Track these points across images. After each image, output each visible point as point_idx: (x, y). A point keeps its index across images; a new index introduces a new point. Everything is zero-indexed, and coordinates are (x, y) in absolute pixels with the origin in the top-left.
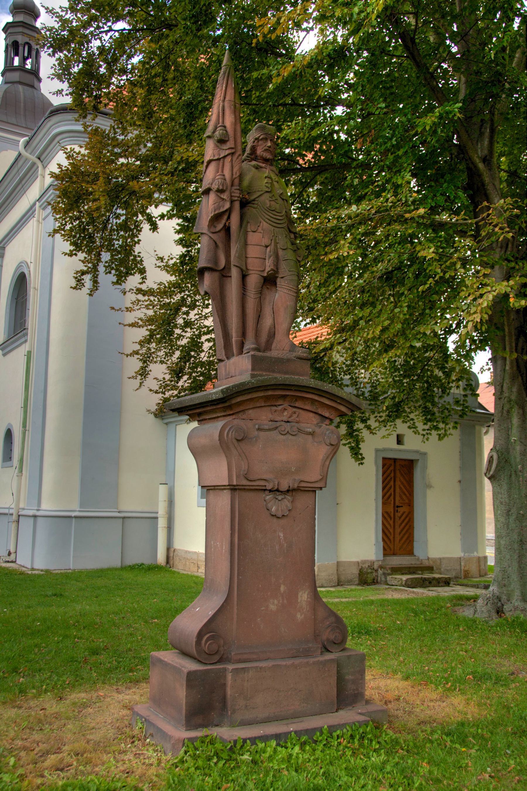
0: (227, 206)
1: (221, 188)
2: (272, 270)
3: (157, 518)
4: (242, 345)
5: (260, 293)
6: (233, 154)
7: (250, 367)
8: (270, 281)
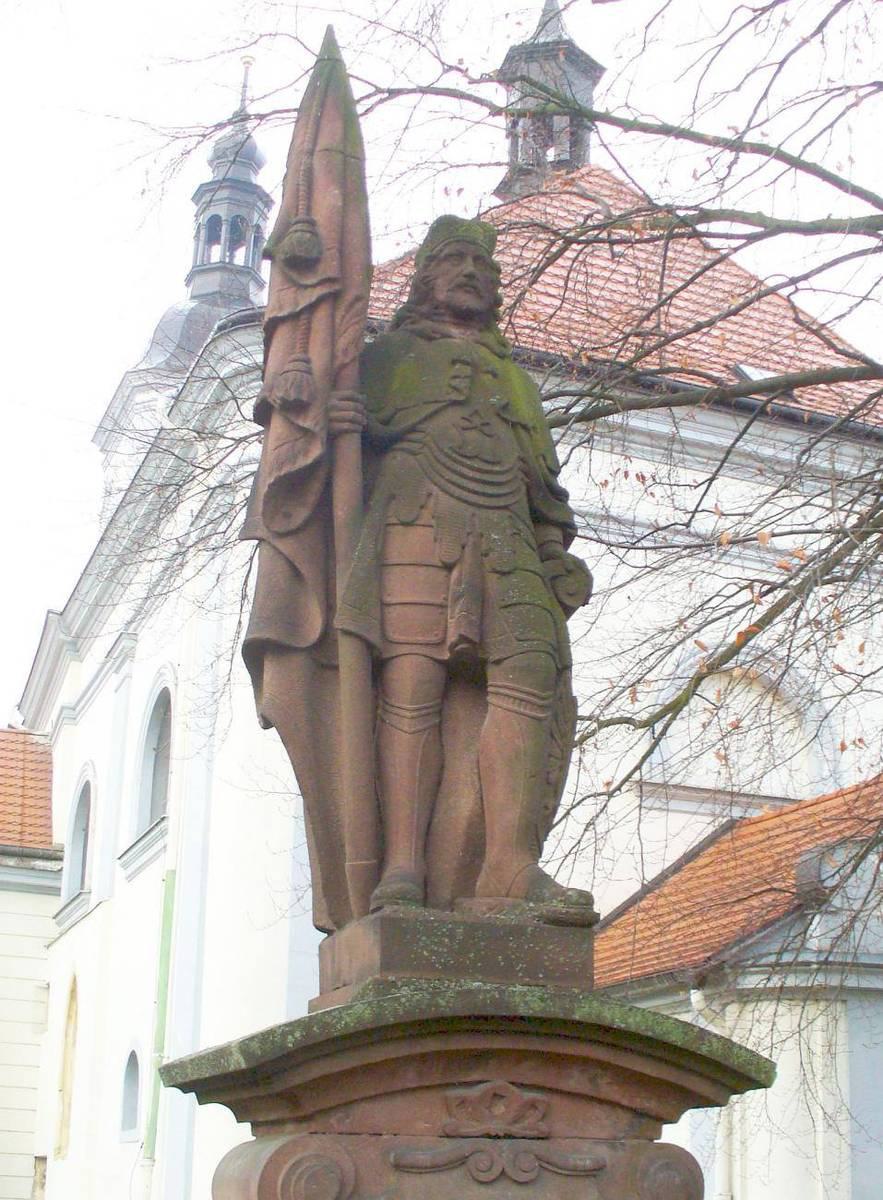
0: (316, 451)
1: (292, 396)
2: (463, 638)
6: (334, 297)
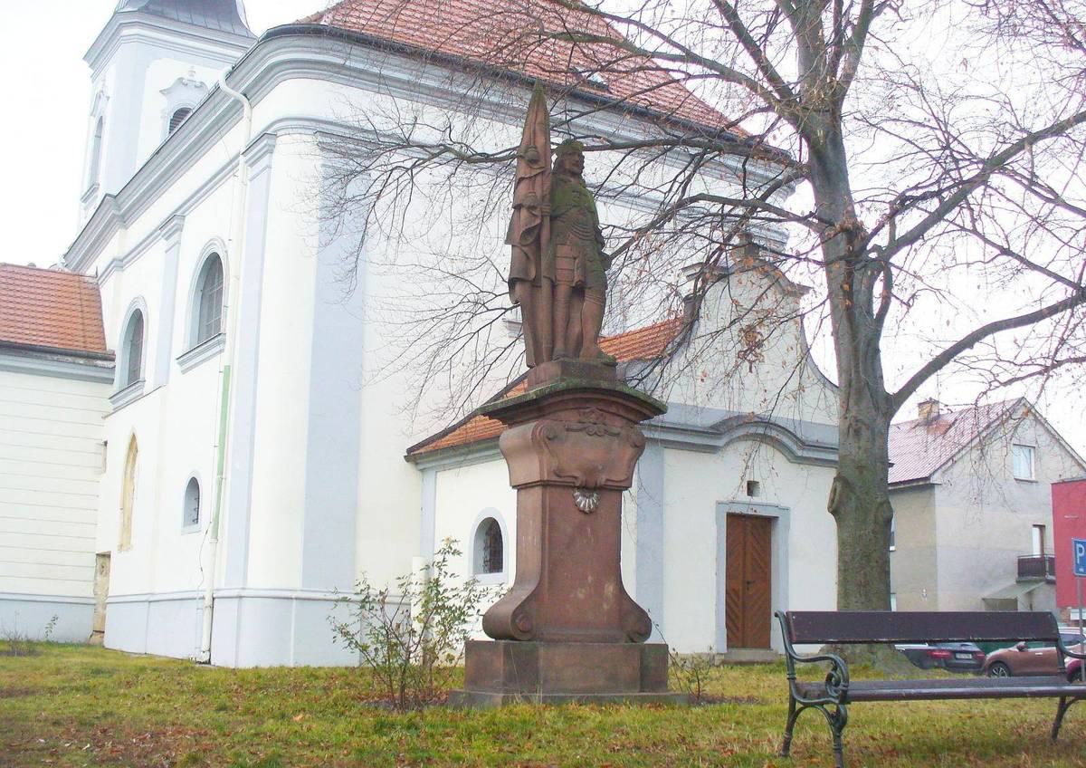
0: (538, 221)
5: (569, 306)
6: (543, 173)
7: (559, 373)
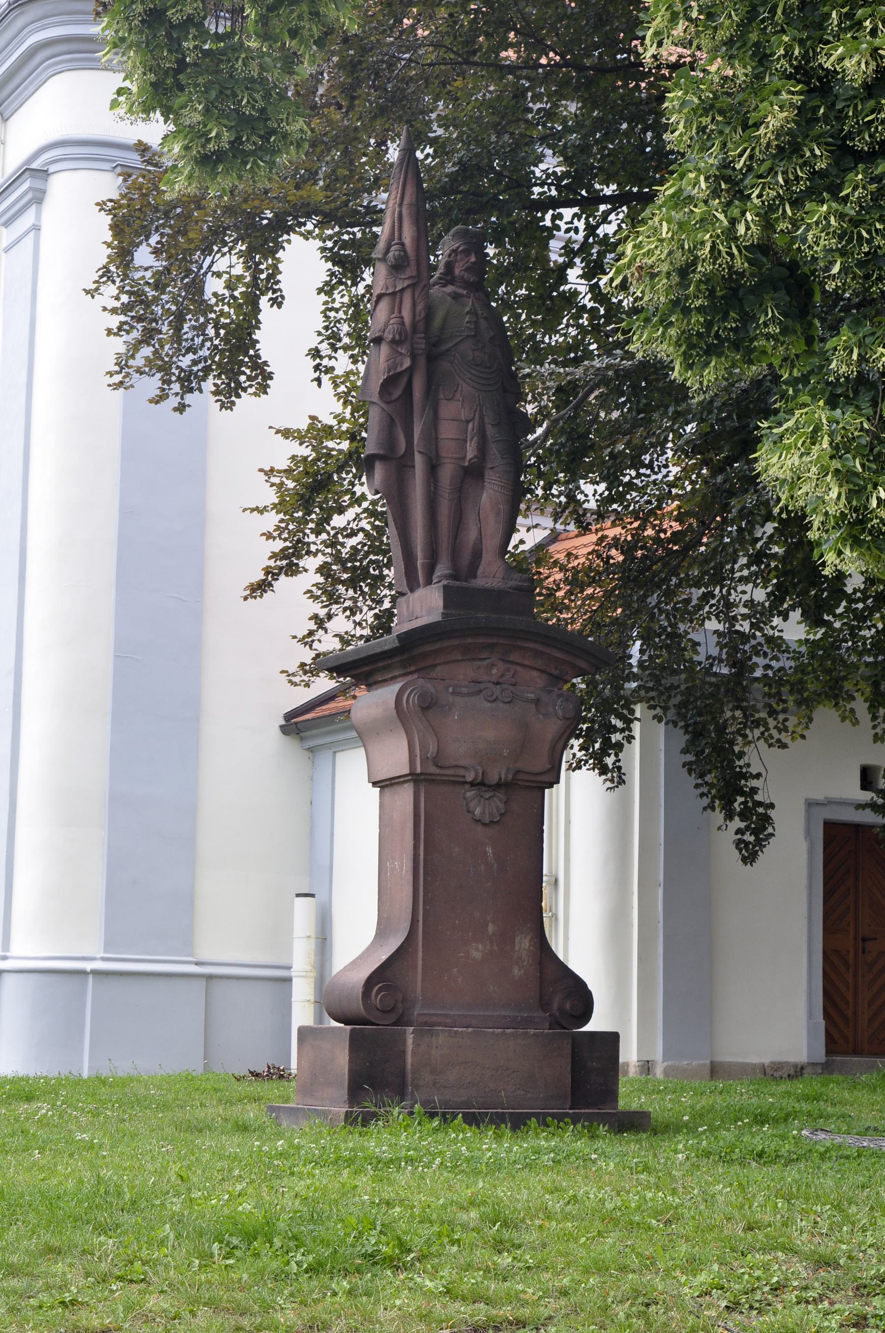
0: (407, 363)
2: (475, 457)
3: (289, 980)
4: (430, 570)
7: (441, 603)
8: (473, 473)
